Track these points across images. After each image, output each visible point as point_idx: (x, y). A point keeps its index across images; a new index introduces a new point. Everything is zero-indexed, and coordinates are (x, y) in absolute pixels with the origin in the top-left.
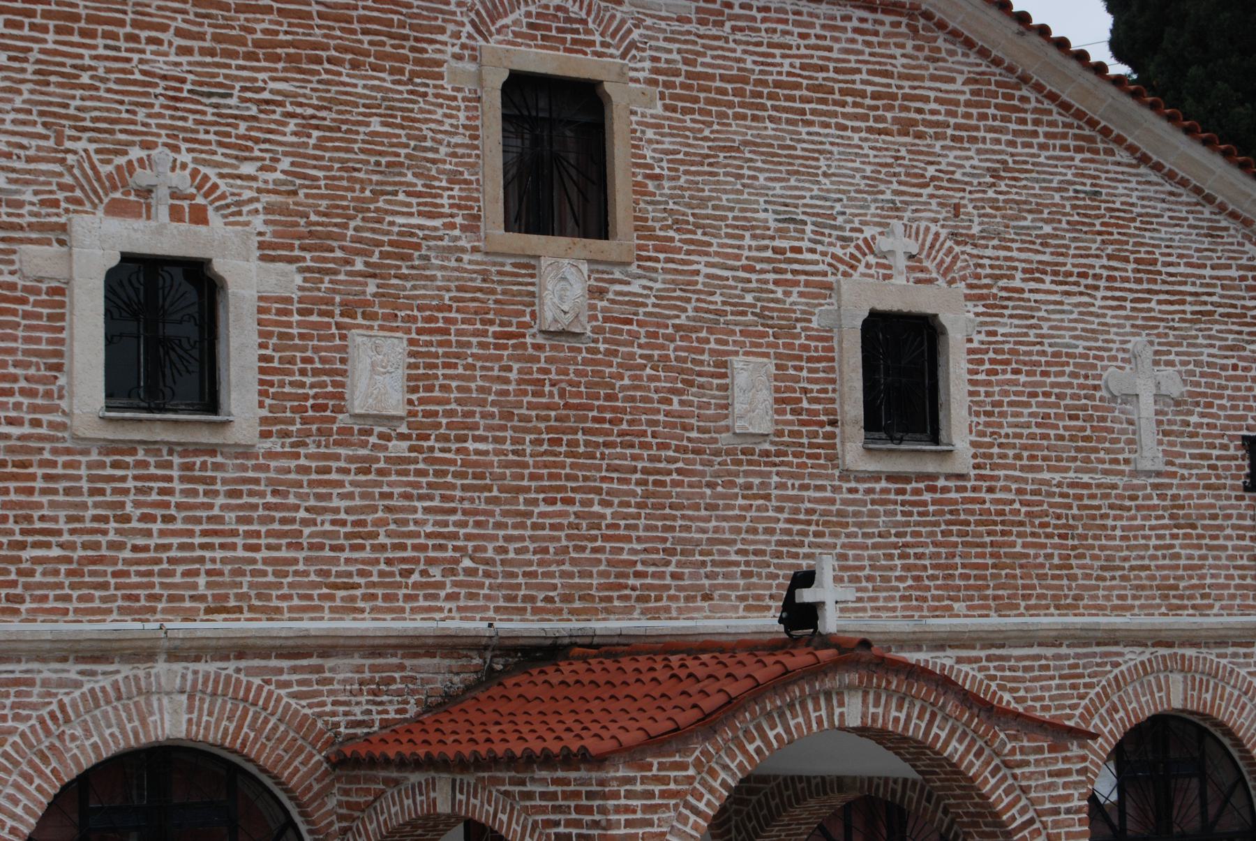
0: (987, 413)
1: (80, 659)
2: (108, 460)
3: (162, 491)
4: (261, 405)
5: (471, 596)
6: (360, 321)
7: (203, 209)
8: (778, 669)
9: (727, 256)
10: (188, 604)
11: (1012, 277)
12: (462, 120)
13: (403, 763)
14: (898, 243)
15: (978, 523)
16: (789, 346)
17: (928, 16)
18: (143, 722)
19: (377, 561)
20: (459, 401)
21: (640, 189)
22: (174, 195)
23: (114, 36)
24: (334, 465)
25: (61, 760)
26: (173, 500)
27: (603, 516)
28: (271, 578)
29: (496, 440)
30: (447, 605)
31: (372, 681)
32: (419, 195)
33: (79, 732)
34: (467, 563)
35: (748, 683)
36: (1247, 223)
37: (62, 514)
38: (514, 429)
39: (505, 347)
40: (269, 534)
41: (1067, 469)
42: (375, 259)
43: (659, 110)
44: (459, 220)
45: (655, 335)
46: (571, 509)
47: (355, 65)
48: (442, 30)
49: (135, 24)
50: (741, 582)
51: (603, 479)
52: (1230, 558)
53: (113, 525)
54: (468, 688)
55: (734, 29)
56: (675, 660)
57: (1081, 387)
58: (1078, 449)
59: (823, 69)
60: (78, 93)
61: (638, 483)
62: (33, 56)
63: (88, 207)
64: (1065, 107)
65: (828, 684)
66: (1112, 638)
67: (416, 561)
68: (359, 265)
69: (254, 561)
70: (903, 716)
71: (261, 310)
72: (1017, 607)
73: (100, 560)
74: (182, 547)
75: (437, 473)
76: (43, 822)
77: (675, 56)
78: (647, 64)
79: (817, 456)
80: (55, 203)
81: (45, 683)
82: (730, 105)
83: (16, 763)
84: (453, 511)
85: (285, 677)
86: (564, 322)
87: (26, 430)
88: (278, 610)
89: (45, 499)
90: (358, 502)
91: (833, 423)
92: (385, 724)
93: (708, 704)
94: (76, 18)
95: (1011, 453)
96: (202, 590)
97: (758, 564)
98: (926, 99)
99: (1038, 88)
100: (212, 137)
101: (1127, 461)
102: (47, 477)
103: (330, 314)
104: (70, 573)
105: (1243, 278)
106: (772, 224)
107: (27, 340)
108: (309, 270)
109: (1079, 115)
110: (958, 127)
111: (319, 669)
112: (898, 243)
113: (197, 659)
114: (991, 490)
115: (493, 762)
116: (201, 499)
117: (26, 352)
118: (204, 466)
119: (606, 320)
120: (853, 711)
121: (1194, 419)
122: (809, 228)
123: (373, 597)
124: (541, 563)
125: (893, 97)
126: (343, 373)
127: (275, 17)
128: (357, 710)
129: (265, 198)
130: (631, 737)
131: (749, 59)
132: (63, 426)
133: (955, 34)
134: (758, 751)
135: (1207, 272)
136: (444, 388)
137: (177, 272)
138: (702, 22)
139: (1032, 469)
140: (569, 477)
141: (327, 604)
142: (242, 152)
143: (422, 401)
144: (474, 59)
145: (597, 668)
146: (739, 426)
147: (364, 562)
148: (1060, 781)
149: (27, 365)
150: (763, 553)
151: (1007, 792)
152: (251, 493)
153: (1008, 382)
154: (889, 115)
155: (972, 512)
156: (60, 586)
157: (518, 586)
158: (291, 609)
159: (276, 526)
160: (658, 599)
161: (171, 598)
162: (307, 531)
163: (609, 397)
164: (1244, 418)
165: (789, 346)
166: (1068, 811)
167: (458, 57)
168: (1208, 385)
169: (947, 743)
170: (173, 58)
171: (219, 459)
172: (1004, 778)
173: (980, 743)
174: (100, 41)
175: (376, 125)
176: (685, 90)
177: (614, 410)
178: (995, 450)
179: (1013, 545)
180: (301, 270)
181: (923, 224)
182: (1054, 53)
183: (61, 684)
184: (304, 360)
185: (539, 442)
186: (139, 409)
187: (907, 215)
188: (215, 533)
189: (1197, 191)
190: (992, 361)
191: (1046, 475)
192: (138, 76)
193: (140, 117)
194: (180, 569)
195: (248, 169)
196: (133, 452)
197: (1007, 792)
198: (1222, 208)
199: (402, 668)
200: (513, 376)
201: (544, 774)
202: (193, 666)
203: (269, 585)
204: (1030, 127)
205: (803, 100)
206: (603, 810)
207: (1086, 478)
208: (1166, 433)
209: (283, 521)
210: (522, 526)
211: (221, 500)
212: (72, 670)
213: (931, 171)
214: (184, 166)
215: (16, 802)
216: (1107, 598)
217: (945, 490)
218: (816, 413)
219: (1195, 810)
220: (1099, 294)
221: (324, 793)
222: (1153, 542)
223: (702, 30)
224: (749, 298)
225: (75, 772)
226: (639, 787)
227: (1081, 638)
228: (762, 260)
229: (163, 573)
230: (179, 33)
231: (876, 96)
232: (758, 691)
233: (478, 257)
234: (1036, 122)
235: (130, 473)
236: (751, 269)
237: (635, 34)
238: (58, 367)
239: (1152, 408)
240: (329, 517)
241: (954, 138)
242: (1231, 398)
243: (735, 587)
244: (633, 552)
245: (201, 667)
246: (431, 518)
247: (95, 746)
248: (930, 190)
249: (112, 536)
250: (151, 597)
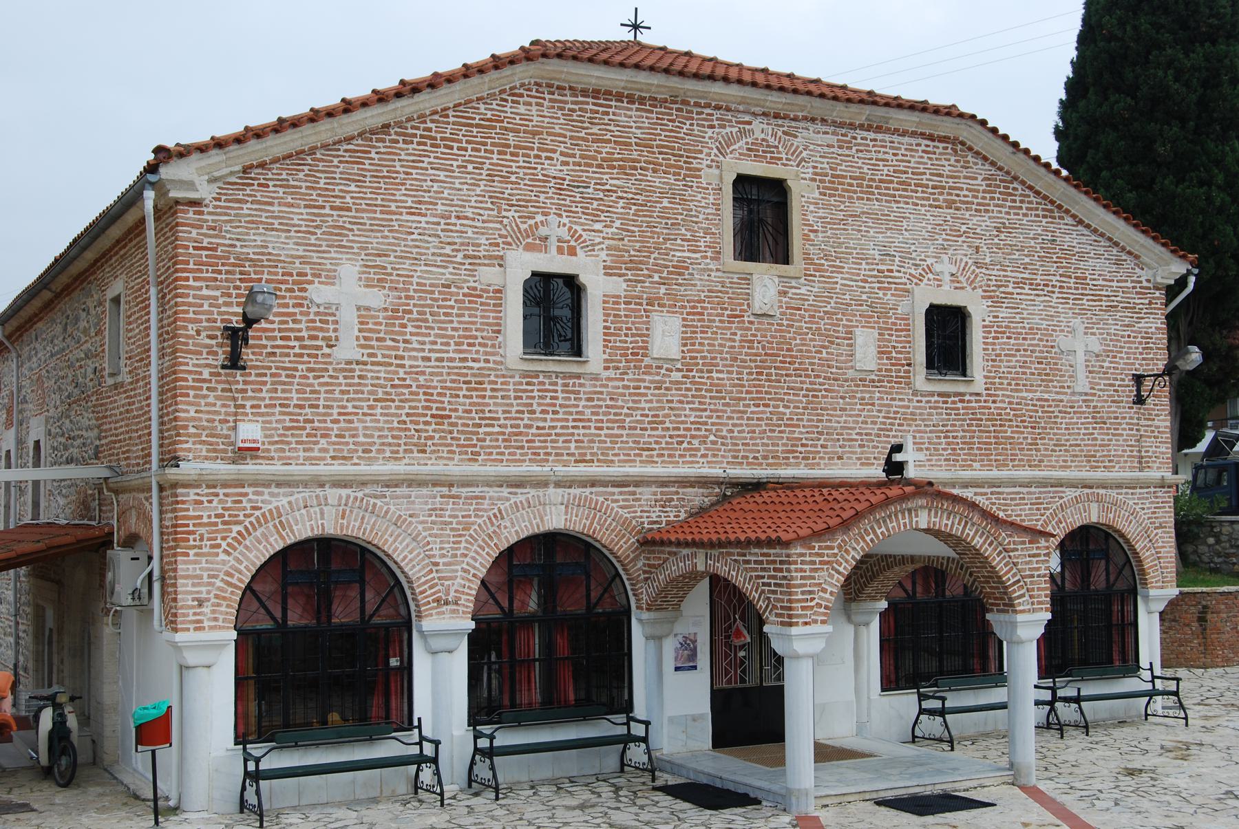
1: (511, 486)
2: (524, 381)
3: (552, 398)
4: (604, 352)
5: (714, 456)
6: (657, 308)
7: (574, 248)
8: (883, 497)
9: (853, 274)
10: (565, 458)
11: (1007, 286)
12: (712, 201)
13: (679, 544)
14: (945, 267)
15: (987, 420)
16: (887, 323)
17: (963, 143)
18: (542, 520)
19: (665, 436)
20: (708, 351)
21: (806, 238)
22: (559, 241)
23: (529, 156)
24: (642, 385)
25: (499, 540)
26: (558, 402)
27: (785, 414)
28: (609, 445)
29: (728, 372)
30: (702, 460)
31: (661, 500)
32: (688, 240)
33: (508, 524)
34: (712, 438)
35: (868, 504)
36: (1137, 257)
37: (500, 409)
38: (738, 366)
39: (733, 322)
40: (608, 421)
41: (1036, 391)
42: (665, 275)
43: (817, 195)
44: (709, 254)
45: (813, 317)
46: (768, 410)
47: (655, 171)
48: (701, 152)
49: (539, 149)
50: (859, 450)
51: (785, 394)
53: (526, 415)
54: (712, 505)
55: (857, 151)
56: (825, 491)
57: (1045, 346)
58: (1042, 380)
59: (905, 172)
60: (510, 186)
61: (804, 396)
62: (486, 166)
63: (514, 246)
64: (1038, 193)
65: (910, 505)
66: (1059, 484)
67: (686, 436)
68: (656, 278)
69: (600, 435)
70: (950, 523)
71: (604, 302)
72: (1007, 465)
73: (520, 434)
74: (562, 427)
75: (696, 390)
76: (489, 571)
77: (825, 166)
78: (811, 170)
79: (900, 383)
80: (497, 245)
81: (491, 498)
82: (855, 192)
83: (476, 540)
84: (705, 410)
85: (616, 497)
86: (765, 310)
87: (482, 364)
88: (612, 461)
89: (491, 401)
90: (655, 405)
91: (909, 365)
92: (668, 523)
93: (845, 515)
94: (508, 146)
95: (1005, 382)
96: (573, 451)
97: (867, 441)
98: (962, 189)
99: (1023, 183)
100: (579, 209)
101: (1069, 387)
102: (493, 390)
103: (641, 304)
104: (505, 440)
105: (1134, 288)
106: (877, 257)
107: (482, 317)
108: (630, 280)
109: (1045, 197)
110: (978, 204)
111: (634, 493)
112: (945, 267)
113: (570, 487)
114: (994, 402)
115: (729, 543)
116: (573, 402)
117: (482, 324)
118: (574, 384)
119: (787, 308)
120: (923, 520)
121: (1106, 364)
122: (897, 259)
123: (663, 455)
124: (751, 438)
125: (944, 188)
126: (648, 336)
127: (612, 145)
128: (654, 515)
129: (607, 242)
130: (804, 532)
131: (866, 167)
132: (502, 363)
133: (977, 153)
134: (872, 540)
135: (1115, 284)
136: (700, 344)
137: (560, 281)
138: (840, 147)
139: (1017, 391)
140: (766, 393)
141: (638, 459)
142: (595, 218)
143: (689, 351)
144: (718, 167)
145: (783, 495)
147: (658, 436)
148: (1034, 559)
149: (483, 330)
150: (870, 434)
151: (1006, 565)
152: (599, 399)
153: (1004, 343)
154: (941, 198)
155: (984, 414)
156: (499, 447)
157: (739, 451)
158: (619, 461)
159: (612, 417)
160: (814, 458)
161: (557, 455)
162: (628, 420)
163: (788, 350)
164: (1133, 364)
165: (887, 323)
166: (1039, 576)
167: (710, 167)
168: (1115, 346)
169: (973, 538)
170: (559, 167)
171: (582, 381)
172: (1004, 558)
173: (991, 538)
174: (521, 159)
175: (666, 203)
176: (830, 184)
177: (791, 356)
178: (997, 380)
179: (1006, 432)
180: (625, 281)
181: (959, 257)
182: (1032, 163)
183: (499, 499)
184: (628, 329)
185: (751, 373)
186: (540, 354)
187: (950, 252)
188: (580, 420)
189: (1110, 239)
190: (996, 332)
191: (1025, 394)
192: (540, 177)
193: (541, 199)
194: (562, 439)
195: (598, 226)
196: (537, 377)
197: (1006, 565)
198: (1123, 249)
199: (677, 493)
200: (738, 338)
201: (756, 550)
202: (568, 490)
203: (608, 448)
204: (1018, 204)
205: (894, 189)
206: (789, 571)
207: (1046, 396)
208: (1090, 372)
209: (615, 414)
210: (742, 418)
211: (583, 403)
212: (505, 491)
213: (964, 228)
214: (564, 225)
215: (476, 560)
216: (1057, 461)
217: (969, 401)
218: (900, 359)
219: (1103, 577)
220: (1055, 296)
221: (636, 558)
222: (1083, 431)
223: (840, 152)
224: (864, 297)
225: (506, 546)
226: (808, 559)
227: (1042, 483)
228: (871, 276)
229: (552, 441)
230: (562, 154)
231: (934, 187)
232: (872, 508)
233: (719, 274)
234: (1021, 202)
235: (535, 388)
236: (866, 282)
237: (804, 154)
238: (499, 332)
239: (1084, 358)
240: (640, 412)
241: (976, 210)
242: (1127, 353)
243: (855, 453)
244: (801, 433)
245: (572, 491)
246: (694, 413)
247: (517, 532)
248: (963, 239)
249: (526, 421)
250: (546, 454)
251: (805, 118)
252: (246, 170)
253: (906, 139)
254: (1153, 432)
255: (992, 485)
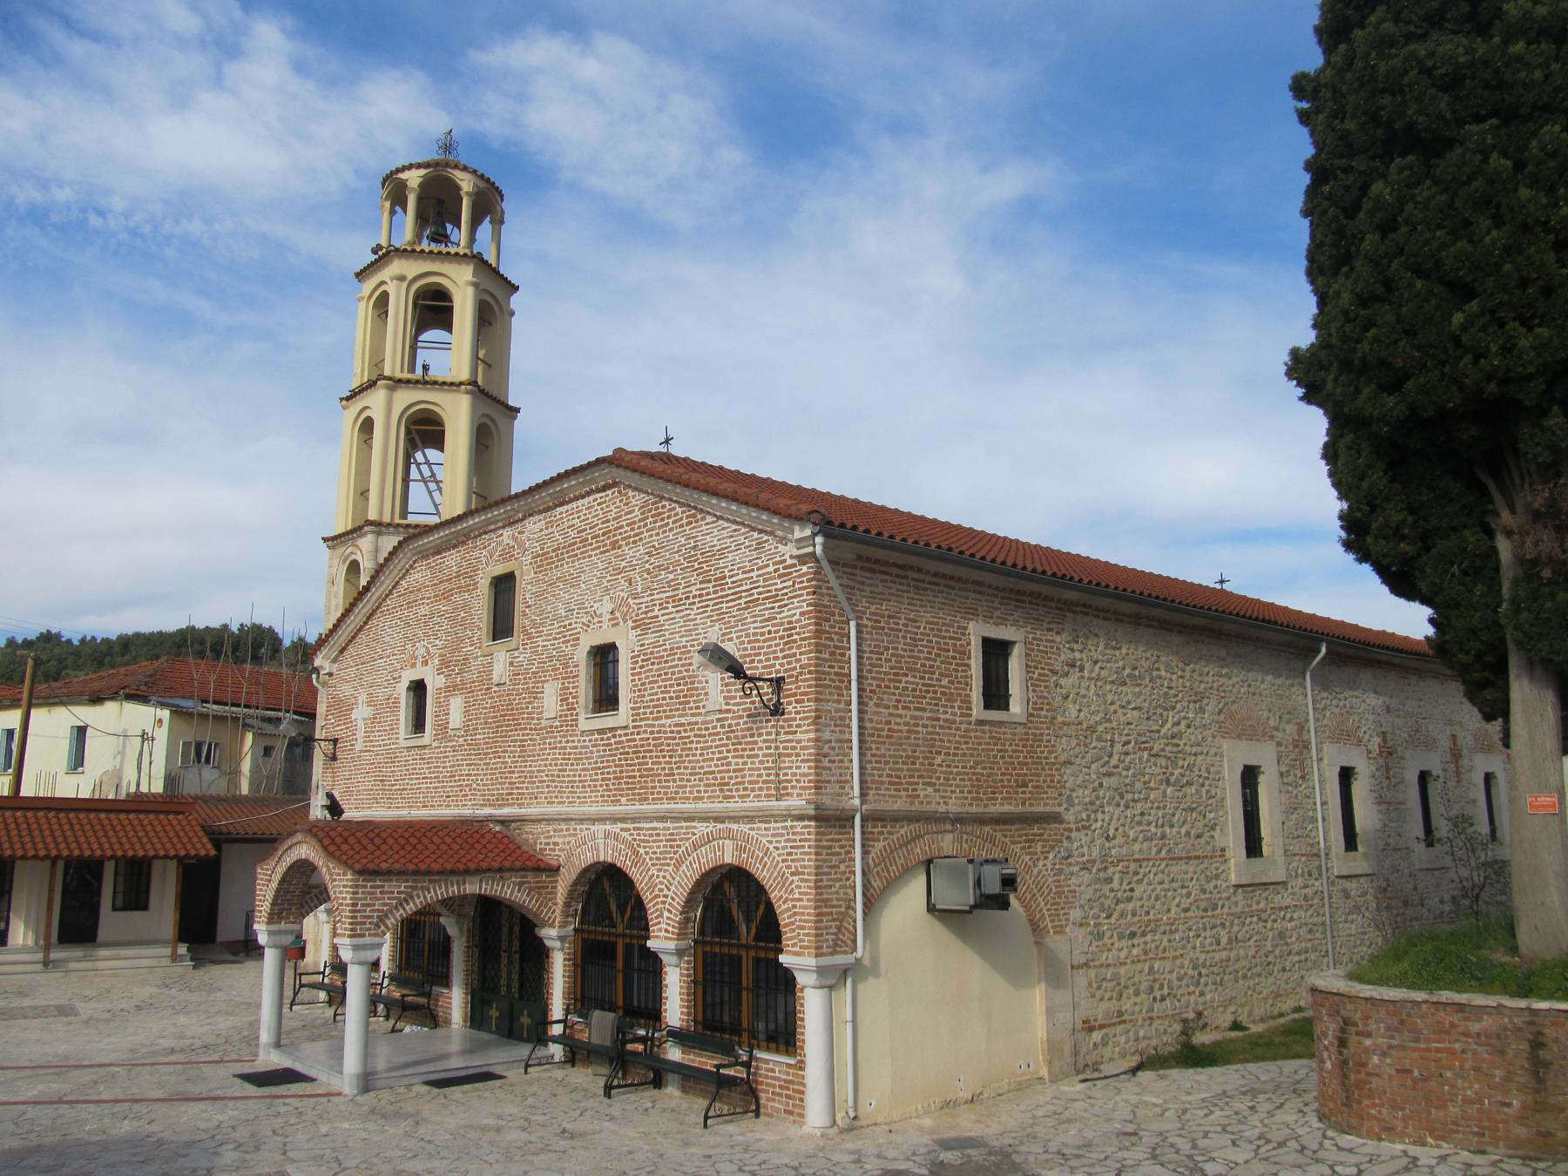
0: (639, 690)
52: (761, 762)
146: (546, 715)
176: (543, 561)
191: (663, 721)
207: (683, 720)
251: (524, 518)
252: (342, 651)
253: (587, 500)
254: (794, 748)
255: (634, 820)
